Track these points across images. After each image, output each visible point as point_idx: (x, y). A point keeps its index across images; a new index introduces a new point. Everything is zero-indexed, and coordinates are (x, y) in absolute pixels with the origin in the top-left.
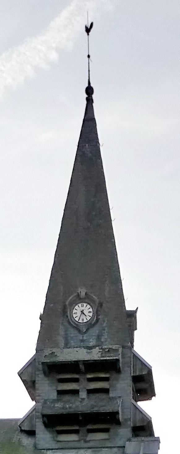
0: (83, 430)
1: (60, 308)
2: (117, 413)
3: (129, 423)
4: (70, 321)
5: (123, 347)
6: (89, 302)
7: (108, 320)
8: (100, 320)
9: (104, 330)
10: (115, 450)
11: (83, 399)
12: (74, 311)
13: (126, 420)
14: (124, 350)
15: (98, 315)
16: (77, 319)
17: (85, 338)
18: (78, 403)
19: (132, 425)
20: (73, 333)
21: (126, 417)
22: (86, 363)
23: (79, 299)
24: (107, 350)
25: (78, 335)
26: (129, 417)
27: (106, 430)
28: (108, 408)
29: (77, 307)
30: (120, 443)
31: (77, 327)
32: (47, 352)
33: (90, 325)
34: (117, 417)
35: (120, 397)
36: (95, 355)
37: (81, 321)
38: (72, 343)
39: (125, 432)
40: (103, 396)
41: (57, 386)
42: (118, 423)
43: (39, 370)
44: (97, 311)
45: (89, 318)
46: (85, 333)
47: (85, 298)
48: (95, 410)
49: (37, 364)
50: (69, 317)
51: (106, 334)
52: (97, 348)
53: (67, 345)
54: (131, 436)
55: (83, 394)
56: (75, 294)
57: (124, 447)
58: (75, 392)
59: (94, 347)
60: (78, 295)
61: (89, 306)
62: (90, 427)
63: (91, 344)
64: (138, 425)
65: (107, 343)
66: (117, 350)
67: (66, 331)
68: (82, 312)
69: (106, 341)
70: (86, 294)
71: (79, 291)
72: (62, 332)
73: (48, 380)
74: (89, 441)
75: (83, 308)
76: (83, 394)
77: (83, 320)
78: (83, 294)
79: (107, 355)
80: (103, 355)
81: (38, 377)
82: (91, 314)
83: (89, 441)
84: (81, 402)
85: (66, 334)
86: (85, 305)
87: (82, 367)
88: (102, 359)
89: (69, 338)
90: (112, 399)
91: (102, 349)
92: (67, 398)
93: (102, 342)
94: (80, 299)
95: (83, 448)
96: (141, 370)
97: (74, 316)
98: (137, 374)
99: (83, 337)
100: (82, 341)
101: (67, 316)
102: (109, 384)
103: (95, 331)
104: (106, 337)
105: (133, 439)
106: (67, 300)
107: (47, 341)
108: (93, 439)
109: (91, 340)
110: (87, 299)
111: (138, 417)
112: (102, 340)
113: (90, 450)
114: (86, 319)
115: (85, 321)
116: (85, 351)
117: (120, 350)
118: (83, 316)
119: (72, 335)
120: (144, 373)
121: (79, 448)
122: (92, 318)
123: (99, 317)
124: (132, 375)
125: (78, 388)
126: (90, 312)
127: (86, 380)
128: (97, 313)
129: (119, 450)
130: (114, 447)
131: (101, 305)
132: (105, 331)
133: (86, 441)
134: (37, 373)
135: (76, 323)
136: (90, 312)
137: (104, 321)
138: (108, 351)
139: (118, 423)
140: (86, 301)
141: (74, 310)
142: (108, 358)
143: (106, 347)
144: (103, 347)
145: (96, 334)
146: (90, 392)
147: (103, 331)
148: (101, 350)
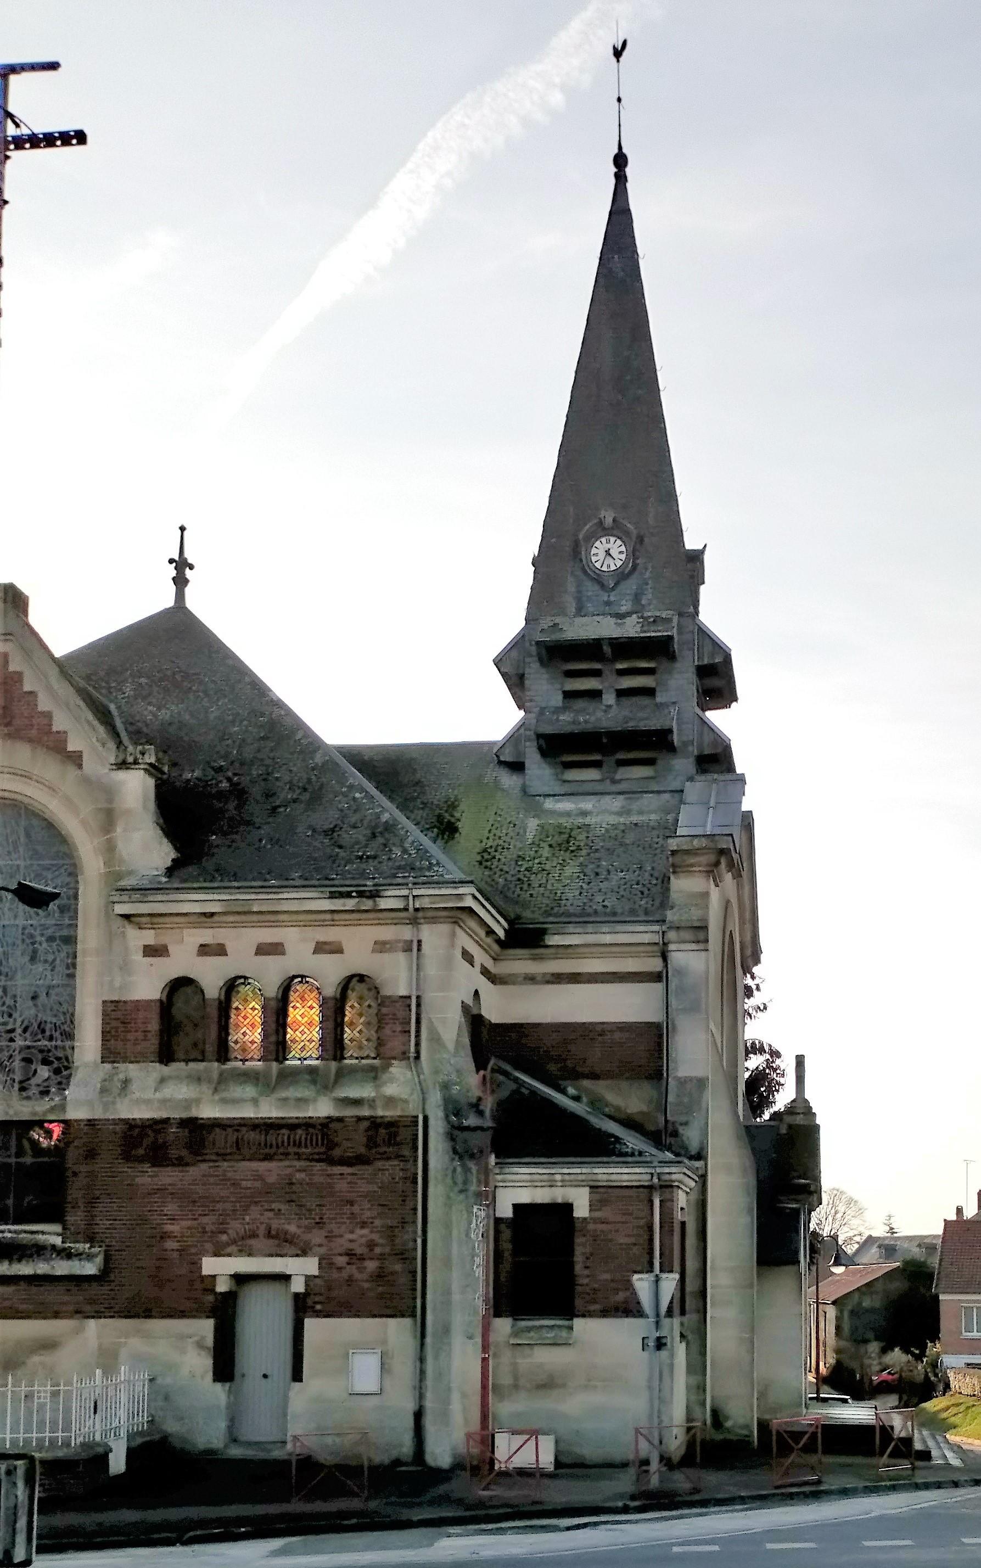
0: (610, 761)
1: (567, 544)
2: (670, 731)
3: (690, 748)
4: (587, 568)
5: (681, 615)
6: (620, 535)
7: (653, 567)
8: (639, 567)
9: (647, 584)
10: (667, 796)
11: (610, 706)
12: (594, 551)
13: (685, 744)
14: (682, 620)
15: (635, 558)
16: (598, 565)
17: (612, 599)
18: (600, 714)
19: (696, 753)
20: (591, 589)
21: (685, 739)
22: (614, 642)
23: (603, 530)
24: (652, 619)
25: (601, 592)
26: (691, 738)
27: (650, 762)
28: (654, 723)
29: (597, 544)
30: (675, 785)
31: (598, 579)
32: (546, 623)
33: (622, 575)
34: (669, 738)
35: (674, 703)
36: (631, 628)
37: (605, 568)
38: (590, 607)
39: (683, 765)
40: (645, 701)
41: (562, 684)
42: (671, 749)
43: (531, 656)
44: (634, 551)
45: (619, 563)
46: (613, 589)
47: (612, 528)
48: (631, 725)
49: (527, 644)
50: (584, 562)
51: (650, 591)
52: (634, 616)
53: (580, 611)
54: (694, 771)
55: (609, 698)
56: (596, 521)
57: (682, 791)
58: (595, 695)
59: (629, 614)
60: (601, 523)
61: (619, 542)
62: (621, 756)
63: (624, 609)
64: (706, 753)
65: (651, 607)
66: (668, 620)
67: (578, 586)
68: (608, 553)
69: (649, 604)
70: (614, 520)
71: (602, 516)
72: (571, 587)
73: (547, 673)
74: (620, 781)
75: (608, 546)
76: (609, 698)
77: (609, 566)
78: (609, 521)
79: (652, 628)
80: (645, 628)
81: (530, 667)
82: (623, 557)
83: (620, 781)
84: (605, 711)
85: (579, 592)
86: (612, 539)
87: (607, 649)
88: (642, 635)
89: (584, 599)
90: (660, 706)
91: (642, 617)
92: (580, 704)
93: (643, 606)
94: (604, 529)
95: (609, 794)
96: (712, 655)
97: (594, 559)
98: (706, 662)
99: (609, 596)
100: (608, 603)
101: (581, 560)
102: (656, 680)
103: (630, 586)
104: (650, 596)
105: (698, 778)
106: (580, 531)
107: (545, 603)
108: (627, 777)
109: (624, 602)
110: (616, 530)
111: (707, 739)
112: (643, 602)
113: (622, 797)
114: (614, 565)
115: (613, 568)
116: (612, 621)
117: (675, 619)
118: (609, 560)
119: (590, 594)
120: (717, 661)
121: (602, 794)
122: (625, 563)
123: (638, 561)
124: (696, 663)
125: (600, 687)
126: (621, 552)
127: (614, 673)
128: (633, 554)
129: (673, 797)
130: (665, 792)
131: (641, 539)
132: (649, 586)
133: (614, 782)
134: (528, 660)
135: (597, 571)
136: (621, 552)
137: (646, 569)
138: (654, 621)
139: (671, 749)
140: (615, 532)
141: (594, 548)
142: (653, 634)
143: (649, 614)
144: (645, 615)
145: (633, 592)
146: (621, 693)
147: (645, 587)
148: (641, 620)
